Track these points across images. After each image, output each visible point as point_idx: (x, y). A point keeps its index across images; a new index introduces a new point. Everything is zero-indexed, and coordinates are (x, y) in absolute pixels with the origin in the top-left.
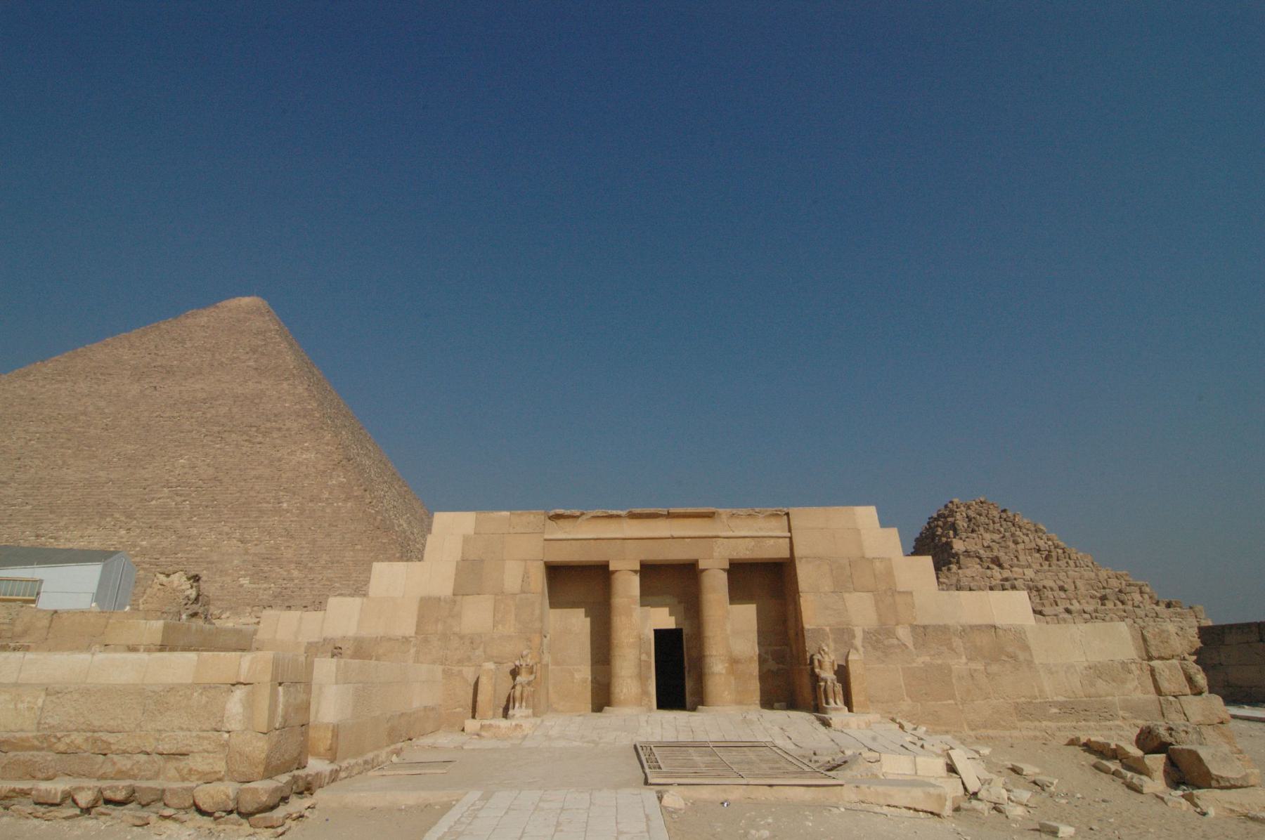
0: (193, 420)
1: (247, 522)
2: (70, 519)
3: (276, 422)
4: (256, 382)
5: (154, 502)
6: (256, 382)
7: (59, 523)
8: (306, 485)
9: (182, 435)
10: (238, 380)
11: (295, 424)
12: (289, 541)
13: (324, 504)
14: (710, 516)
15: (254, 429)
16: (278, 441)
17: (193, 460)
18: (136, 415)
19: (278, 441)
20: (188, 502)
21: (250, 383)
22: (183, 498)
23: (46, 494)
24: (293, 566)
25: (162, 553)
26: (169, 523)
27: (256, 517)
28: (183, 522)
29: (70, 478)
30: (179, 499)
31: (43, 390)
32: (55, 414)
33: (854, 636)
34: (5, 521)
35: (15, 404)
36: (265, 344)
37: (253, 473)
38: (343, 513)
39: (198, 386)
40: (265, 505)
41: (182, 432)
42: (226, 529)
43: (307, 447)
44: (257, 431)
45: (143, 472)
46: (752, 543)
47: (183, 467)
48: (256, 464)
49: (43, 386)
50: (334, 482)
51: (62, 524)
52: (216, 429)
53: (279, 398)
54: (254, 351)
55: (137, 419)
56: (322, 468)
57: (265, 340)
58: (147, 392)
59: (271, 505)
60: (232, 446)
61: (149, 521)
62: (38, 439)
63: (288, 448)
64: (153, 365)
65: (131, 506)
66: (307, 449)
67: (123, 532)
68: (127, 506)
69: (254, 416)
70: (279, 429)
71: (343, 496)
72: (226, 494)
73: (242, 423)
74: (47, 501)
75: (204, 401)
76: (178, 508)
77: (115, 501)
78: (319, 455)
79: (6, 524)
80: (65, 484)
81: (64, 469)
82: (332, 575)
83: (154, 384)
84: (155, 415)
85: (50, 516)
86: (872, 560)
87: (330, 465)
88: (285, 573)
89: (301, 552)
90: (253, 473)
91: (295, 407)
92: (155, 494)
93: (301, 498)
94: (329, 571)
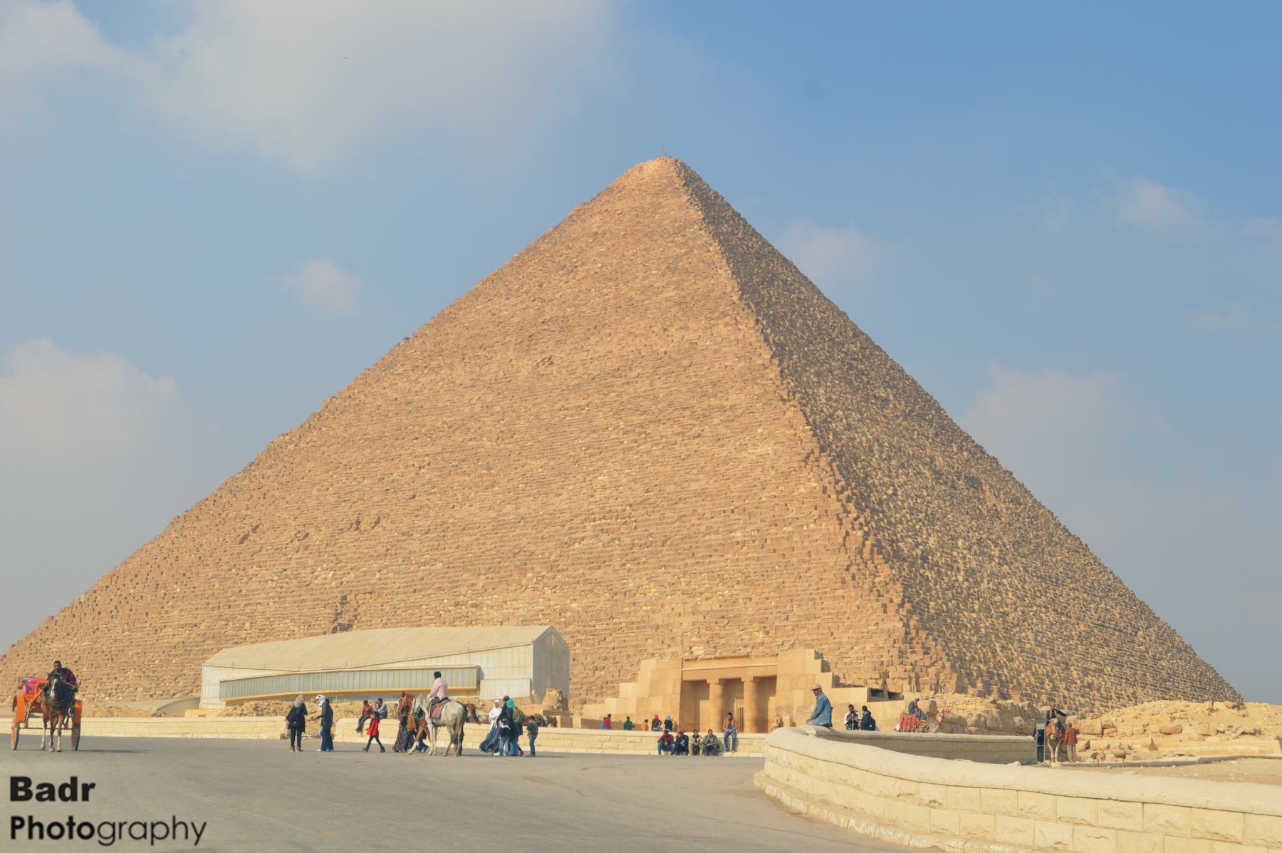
0: (606, 409)
1: (693, 565)
2: (487, 578)
3: (715, 396)
4: (682, 328)
5: (577, 545)
6: (682, 328)
7: (476, 584)
8: (764, 499)
9: (595, 436)
10: (655, 329)
11: (742, 397)
12: (748, 590)
13: (790, 528)
14: (747, 656)
15: (687, 413)
16: (722, 430)
17: (615, 475)
18: (534, 410)
19: (722, 430)
20: (617, 542)
21: (673, 330)
22: (611, 536)
23: (455, 546)
24: (755, 625)
25: (599, 620)
26: (598, 574)
27: (703, 557)
28: (616, 571)
29: (477, 519)
30: (605, 538)
31: (418, 386)
32: (439, 424)
33: (793, 709)
34: (419, 587)
35: (390, 414)
36: (686, 253)
37: (694, 486)
38: (817, 540)
39: (601, 350)
40: (713, 537)
41: (594, 432)
42: (669, 578)
43: (762, 434)
44: (691, 417)
45: (557, 499)
46: (762, 669)
47: (604, 488)
48: (695, 471)
49: (416, 381)
50: (802, 490)
51: (480, 585)
52: (636, 419)
53: (716, 351)
54: (672, 269)
55: (537, 416)
56: (784, 468)
57: (685, 244)
58: (541, 369)
59: (720, 536)
60: (661, 446)
61: (575, 573)
62: (429, 464)
63: (736, 441)
64: (541, 320)
65: (551, 554)
66: (763, 439)
67: (548, 591)
68: (547, 554)
69: (684, 389)
70: (722, 409)
71: (816, 513)
72: (662, 524)
73: (670, 405)
74: (457, 555)
75: (617, 373)
76: (606, 552)
77: (532, 547)
78: (777, 447)
79: (420, 590)
80: (473, 528)
81: (466, 506)
82: (806, 637)
83: (548, 355)
84: (557, 406)
85: (465, 576)
86: (807, 675)
87: (794, 461)
88: (747, 637)
89: (765, 606)
90: (694, 486)
91: (739, 365)
92: (576, 533)
93: (759, 521)
94: (803, 631)
